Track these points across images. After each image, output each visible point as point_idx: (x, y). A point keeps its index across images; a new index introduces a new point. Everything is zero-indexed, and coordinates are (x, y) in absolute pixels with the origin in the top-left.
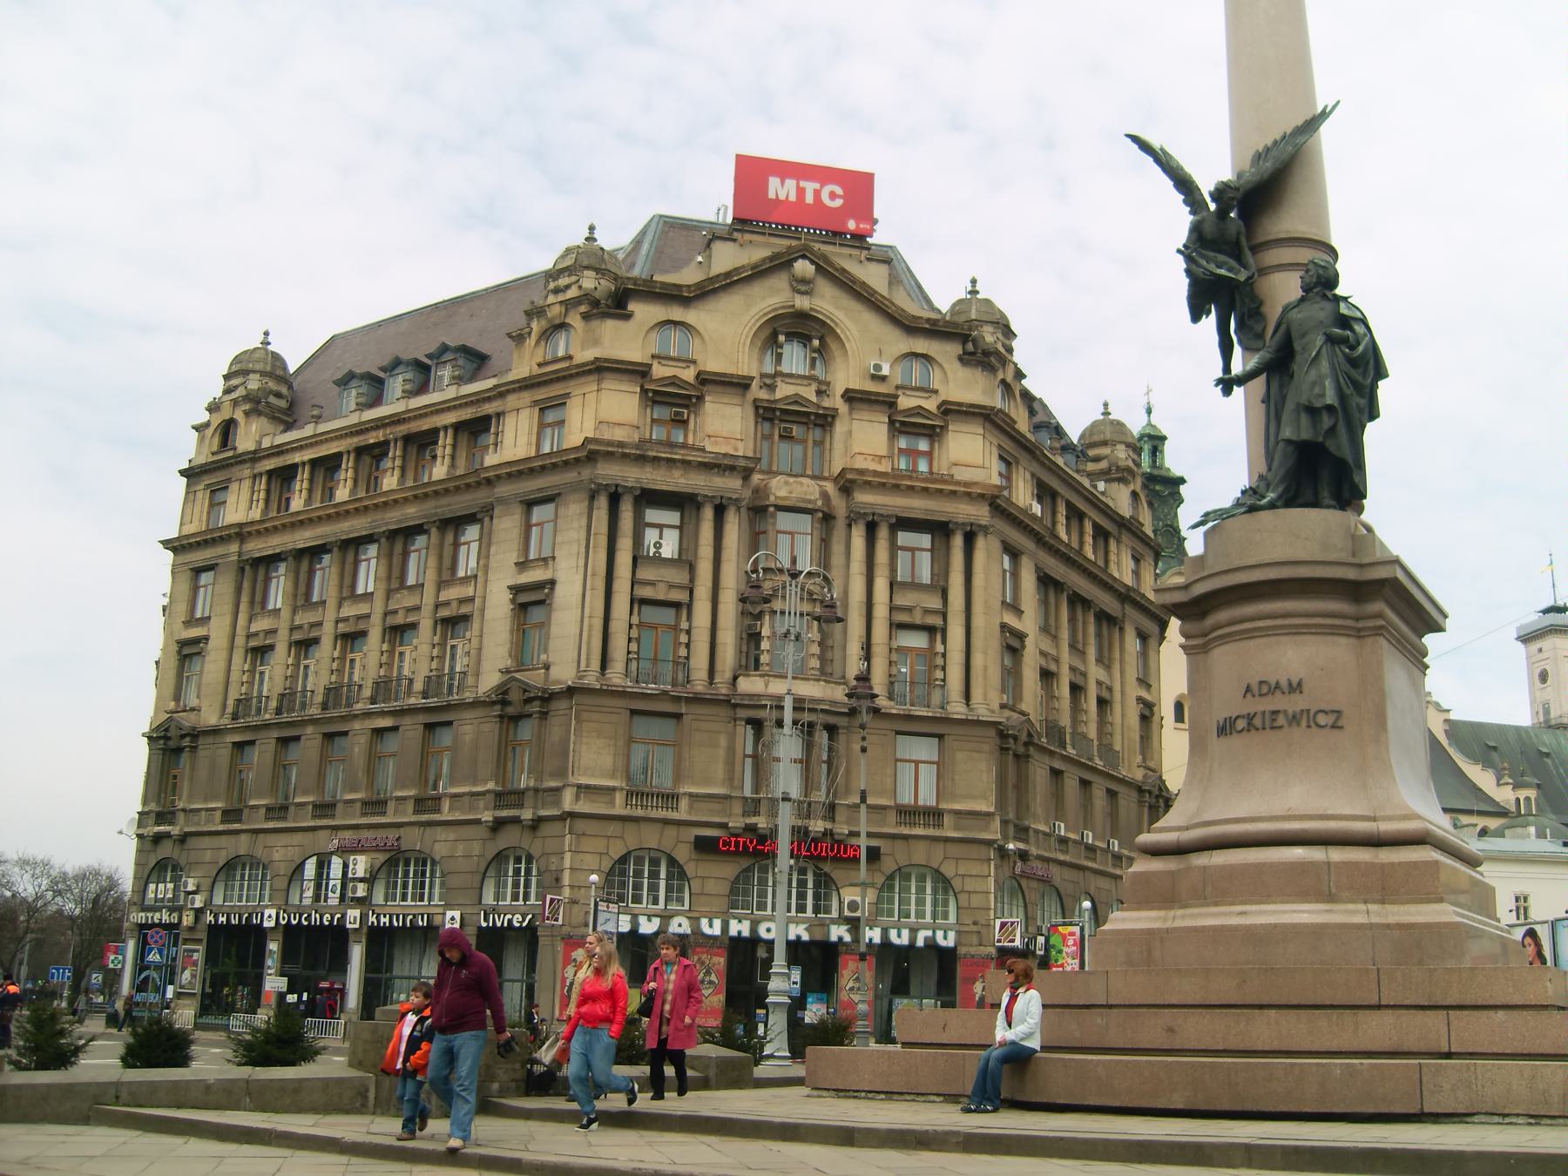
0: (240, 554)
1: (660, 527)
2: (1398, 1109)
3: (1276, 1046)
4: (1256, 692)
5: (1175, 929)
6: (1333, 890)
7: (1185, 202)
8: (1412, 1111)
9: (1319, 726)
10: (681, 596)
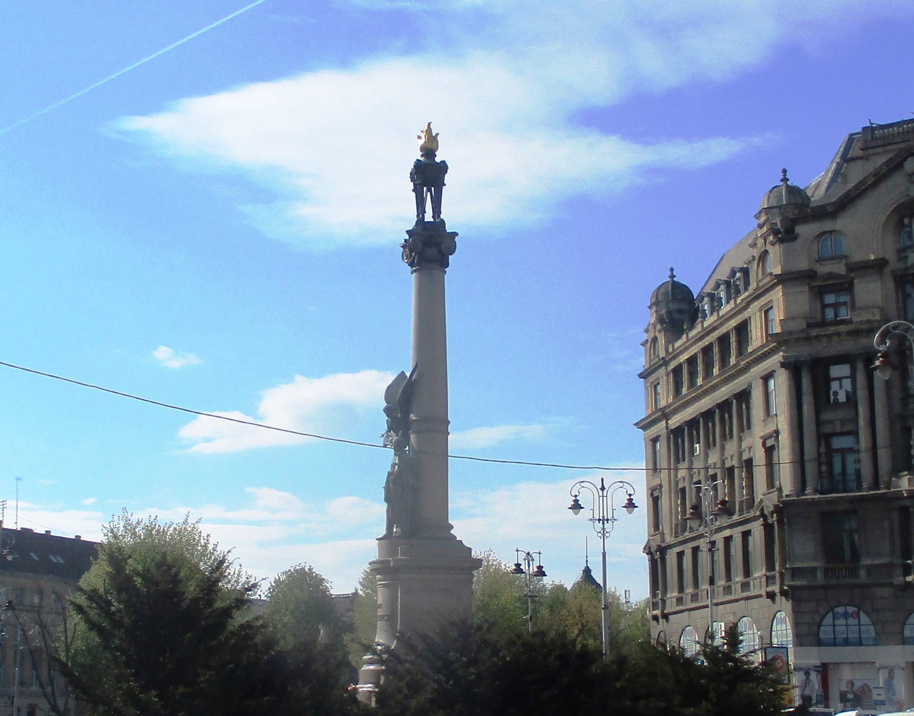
0: (667, 428)
1: (840, 379)
10: (849, 427)
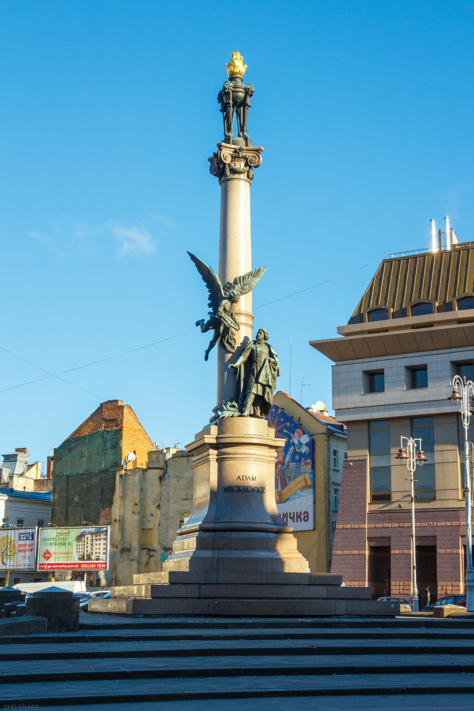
2: (331, 614)
3: (290, 596)
4: (241, 478)
5: (222, 558)
6: (271, 547)
7: (207, 286)
8: (334, 614)
9: (260, 492)
